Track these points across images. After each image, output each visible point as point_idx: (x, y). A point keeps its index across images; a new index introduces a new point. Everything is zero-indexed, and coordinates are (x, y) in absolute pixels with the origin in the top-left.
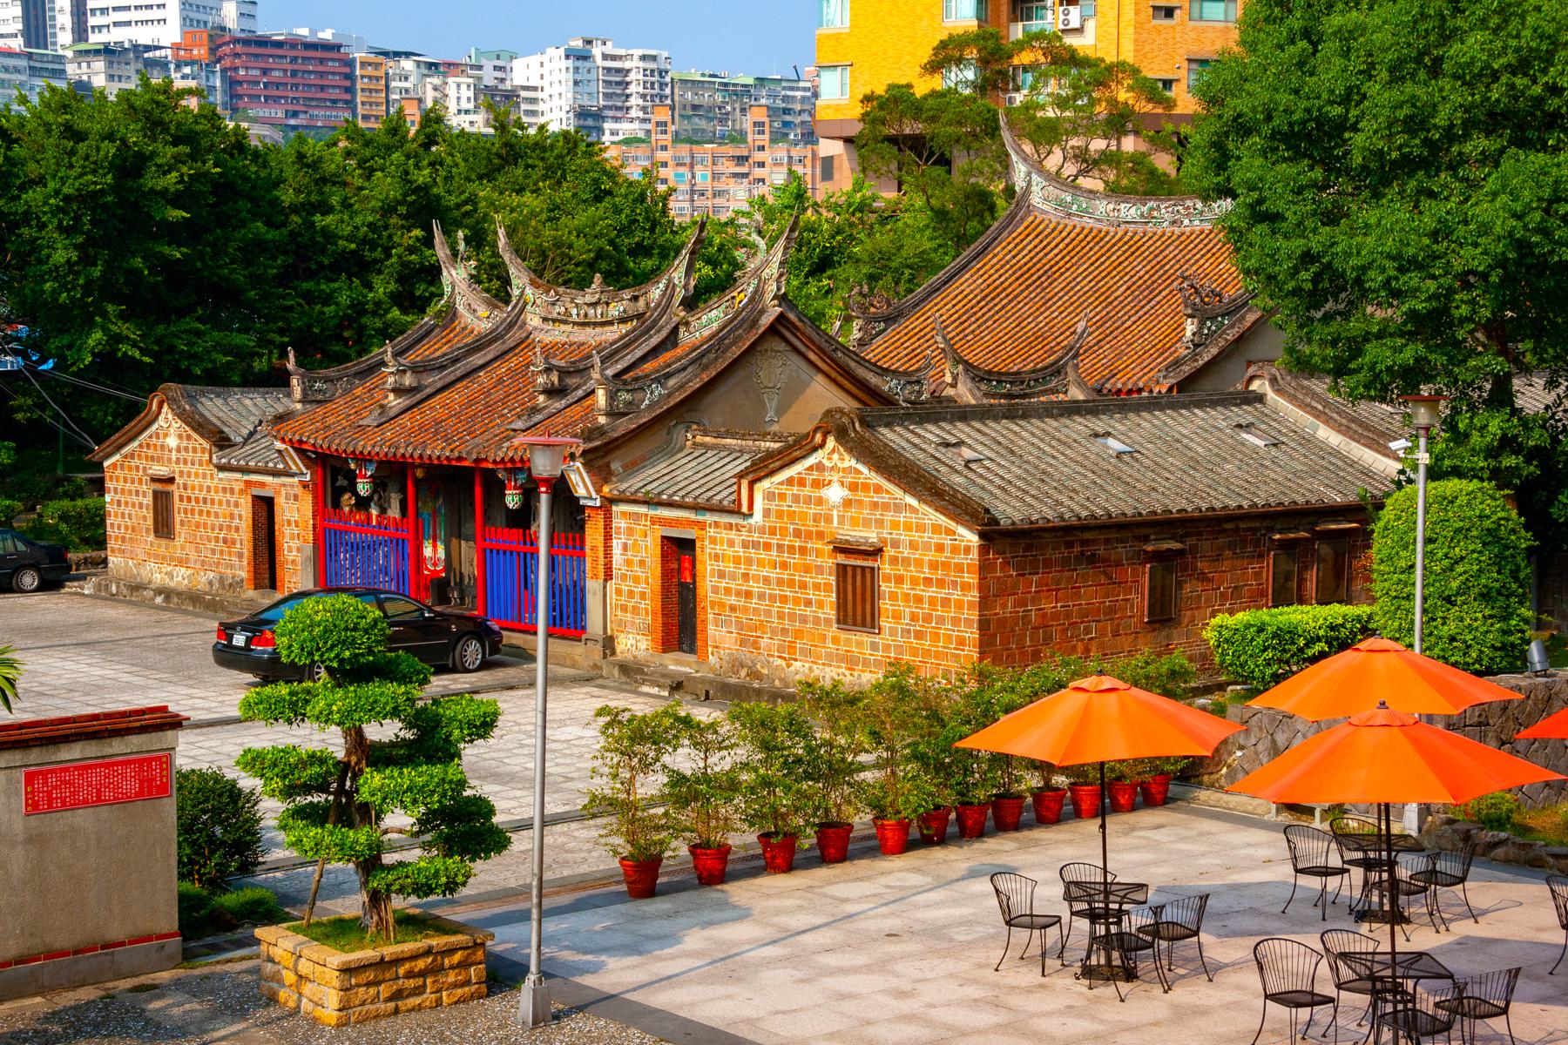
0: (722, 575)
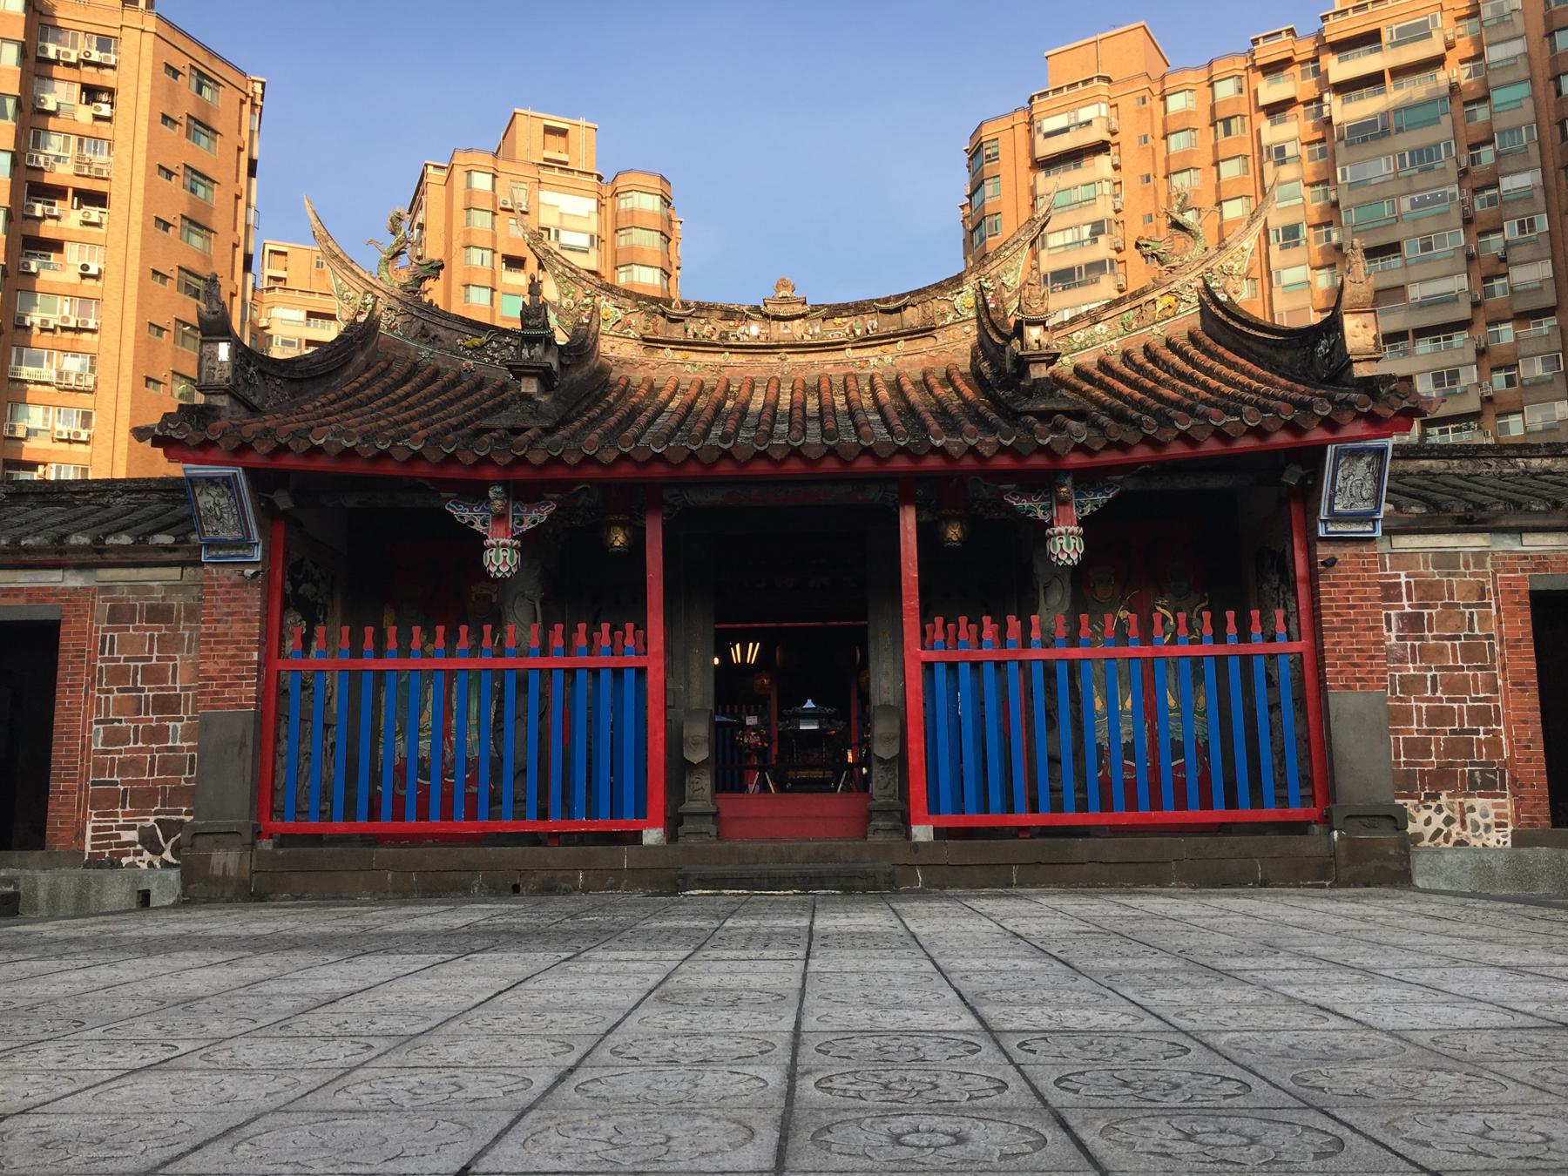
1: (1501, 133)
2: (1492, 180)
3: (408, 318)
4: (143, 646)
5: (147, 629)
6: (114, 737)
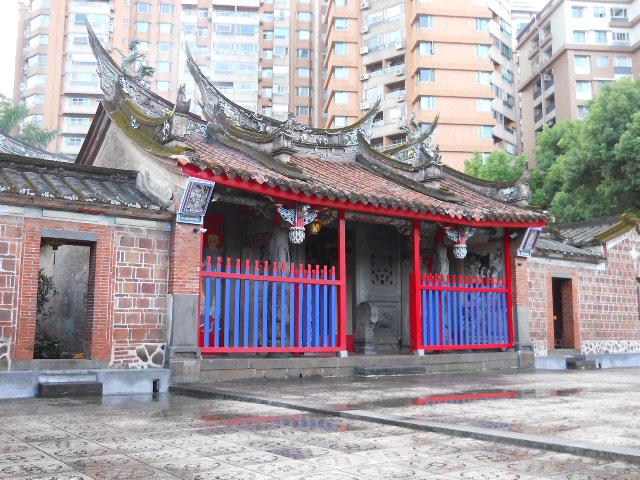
0: (586, 298)
6: (124, 304)
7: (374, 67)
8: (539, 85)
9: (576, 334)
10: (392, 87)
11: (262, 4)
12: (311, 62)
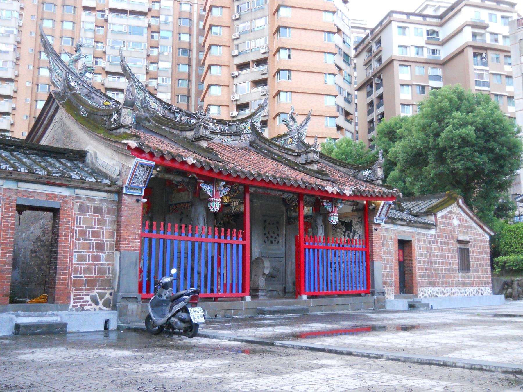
0: (422, 255)
1: (161, 46)
2: (155, 61)
3: (81, 87)
4: (92, 222)
5: (94, 216)
6: (81, 258)
7: (243, 66)
8: (371, 86)
9: (414, 283)
10: (257, 83)
11: (150, 10)
12: (190, 60)
